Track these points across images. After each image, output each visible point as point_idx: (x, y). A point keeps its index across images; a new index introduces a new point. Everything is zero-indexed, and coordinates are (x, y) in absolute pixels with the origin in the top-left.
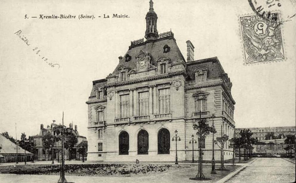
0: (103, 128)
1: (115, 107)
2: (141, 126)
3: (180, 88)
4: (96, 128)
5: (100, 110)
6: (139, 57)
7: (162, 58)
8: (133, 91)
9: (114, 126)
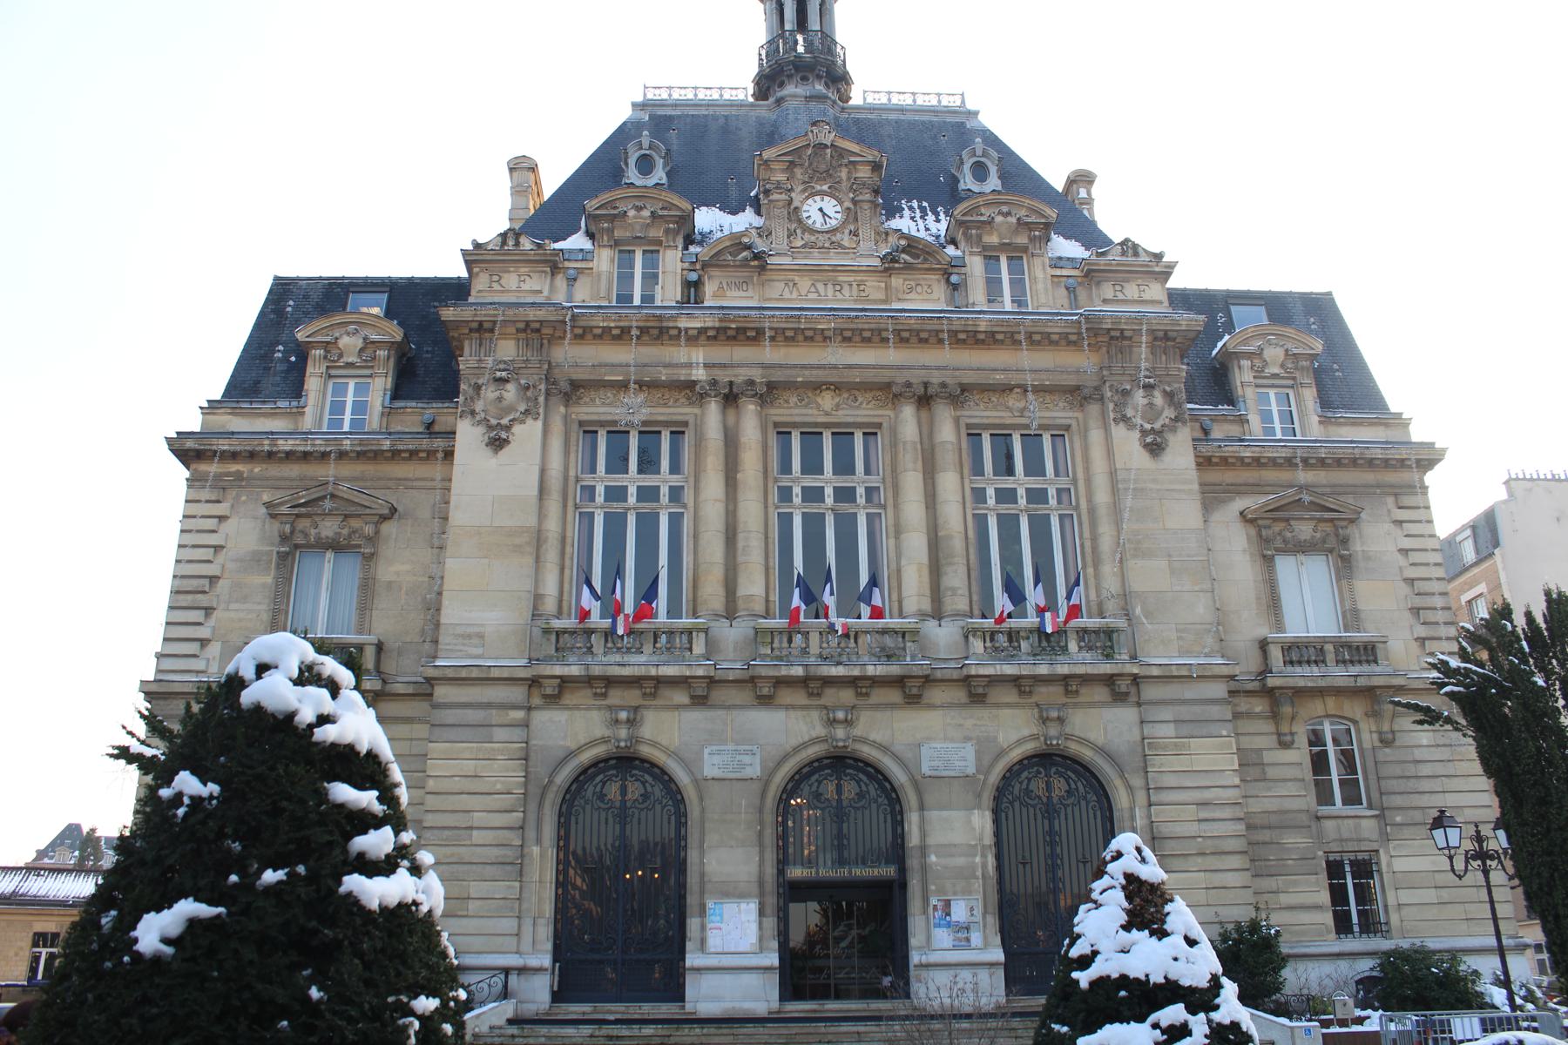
1: (541, 515)
7: (1005, 209)
8: (731, 398)
9: (517, 694)
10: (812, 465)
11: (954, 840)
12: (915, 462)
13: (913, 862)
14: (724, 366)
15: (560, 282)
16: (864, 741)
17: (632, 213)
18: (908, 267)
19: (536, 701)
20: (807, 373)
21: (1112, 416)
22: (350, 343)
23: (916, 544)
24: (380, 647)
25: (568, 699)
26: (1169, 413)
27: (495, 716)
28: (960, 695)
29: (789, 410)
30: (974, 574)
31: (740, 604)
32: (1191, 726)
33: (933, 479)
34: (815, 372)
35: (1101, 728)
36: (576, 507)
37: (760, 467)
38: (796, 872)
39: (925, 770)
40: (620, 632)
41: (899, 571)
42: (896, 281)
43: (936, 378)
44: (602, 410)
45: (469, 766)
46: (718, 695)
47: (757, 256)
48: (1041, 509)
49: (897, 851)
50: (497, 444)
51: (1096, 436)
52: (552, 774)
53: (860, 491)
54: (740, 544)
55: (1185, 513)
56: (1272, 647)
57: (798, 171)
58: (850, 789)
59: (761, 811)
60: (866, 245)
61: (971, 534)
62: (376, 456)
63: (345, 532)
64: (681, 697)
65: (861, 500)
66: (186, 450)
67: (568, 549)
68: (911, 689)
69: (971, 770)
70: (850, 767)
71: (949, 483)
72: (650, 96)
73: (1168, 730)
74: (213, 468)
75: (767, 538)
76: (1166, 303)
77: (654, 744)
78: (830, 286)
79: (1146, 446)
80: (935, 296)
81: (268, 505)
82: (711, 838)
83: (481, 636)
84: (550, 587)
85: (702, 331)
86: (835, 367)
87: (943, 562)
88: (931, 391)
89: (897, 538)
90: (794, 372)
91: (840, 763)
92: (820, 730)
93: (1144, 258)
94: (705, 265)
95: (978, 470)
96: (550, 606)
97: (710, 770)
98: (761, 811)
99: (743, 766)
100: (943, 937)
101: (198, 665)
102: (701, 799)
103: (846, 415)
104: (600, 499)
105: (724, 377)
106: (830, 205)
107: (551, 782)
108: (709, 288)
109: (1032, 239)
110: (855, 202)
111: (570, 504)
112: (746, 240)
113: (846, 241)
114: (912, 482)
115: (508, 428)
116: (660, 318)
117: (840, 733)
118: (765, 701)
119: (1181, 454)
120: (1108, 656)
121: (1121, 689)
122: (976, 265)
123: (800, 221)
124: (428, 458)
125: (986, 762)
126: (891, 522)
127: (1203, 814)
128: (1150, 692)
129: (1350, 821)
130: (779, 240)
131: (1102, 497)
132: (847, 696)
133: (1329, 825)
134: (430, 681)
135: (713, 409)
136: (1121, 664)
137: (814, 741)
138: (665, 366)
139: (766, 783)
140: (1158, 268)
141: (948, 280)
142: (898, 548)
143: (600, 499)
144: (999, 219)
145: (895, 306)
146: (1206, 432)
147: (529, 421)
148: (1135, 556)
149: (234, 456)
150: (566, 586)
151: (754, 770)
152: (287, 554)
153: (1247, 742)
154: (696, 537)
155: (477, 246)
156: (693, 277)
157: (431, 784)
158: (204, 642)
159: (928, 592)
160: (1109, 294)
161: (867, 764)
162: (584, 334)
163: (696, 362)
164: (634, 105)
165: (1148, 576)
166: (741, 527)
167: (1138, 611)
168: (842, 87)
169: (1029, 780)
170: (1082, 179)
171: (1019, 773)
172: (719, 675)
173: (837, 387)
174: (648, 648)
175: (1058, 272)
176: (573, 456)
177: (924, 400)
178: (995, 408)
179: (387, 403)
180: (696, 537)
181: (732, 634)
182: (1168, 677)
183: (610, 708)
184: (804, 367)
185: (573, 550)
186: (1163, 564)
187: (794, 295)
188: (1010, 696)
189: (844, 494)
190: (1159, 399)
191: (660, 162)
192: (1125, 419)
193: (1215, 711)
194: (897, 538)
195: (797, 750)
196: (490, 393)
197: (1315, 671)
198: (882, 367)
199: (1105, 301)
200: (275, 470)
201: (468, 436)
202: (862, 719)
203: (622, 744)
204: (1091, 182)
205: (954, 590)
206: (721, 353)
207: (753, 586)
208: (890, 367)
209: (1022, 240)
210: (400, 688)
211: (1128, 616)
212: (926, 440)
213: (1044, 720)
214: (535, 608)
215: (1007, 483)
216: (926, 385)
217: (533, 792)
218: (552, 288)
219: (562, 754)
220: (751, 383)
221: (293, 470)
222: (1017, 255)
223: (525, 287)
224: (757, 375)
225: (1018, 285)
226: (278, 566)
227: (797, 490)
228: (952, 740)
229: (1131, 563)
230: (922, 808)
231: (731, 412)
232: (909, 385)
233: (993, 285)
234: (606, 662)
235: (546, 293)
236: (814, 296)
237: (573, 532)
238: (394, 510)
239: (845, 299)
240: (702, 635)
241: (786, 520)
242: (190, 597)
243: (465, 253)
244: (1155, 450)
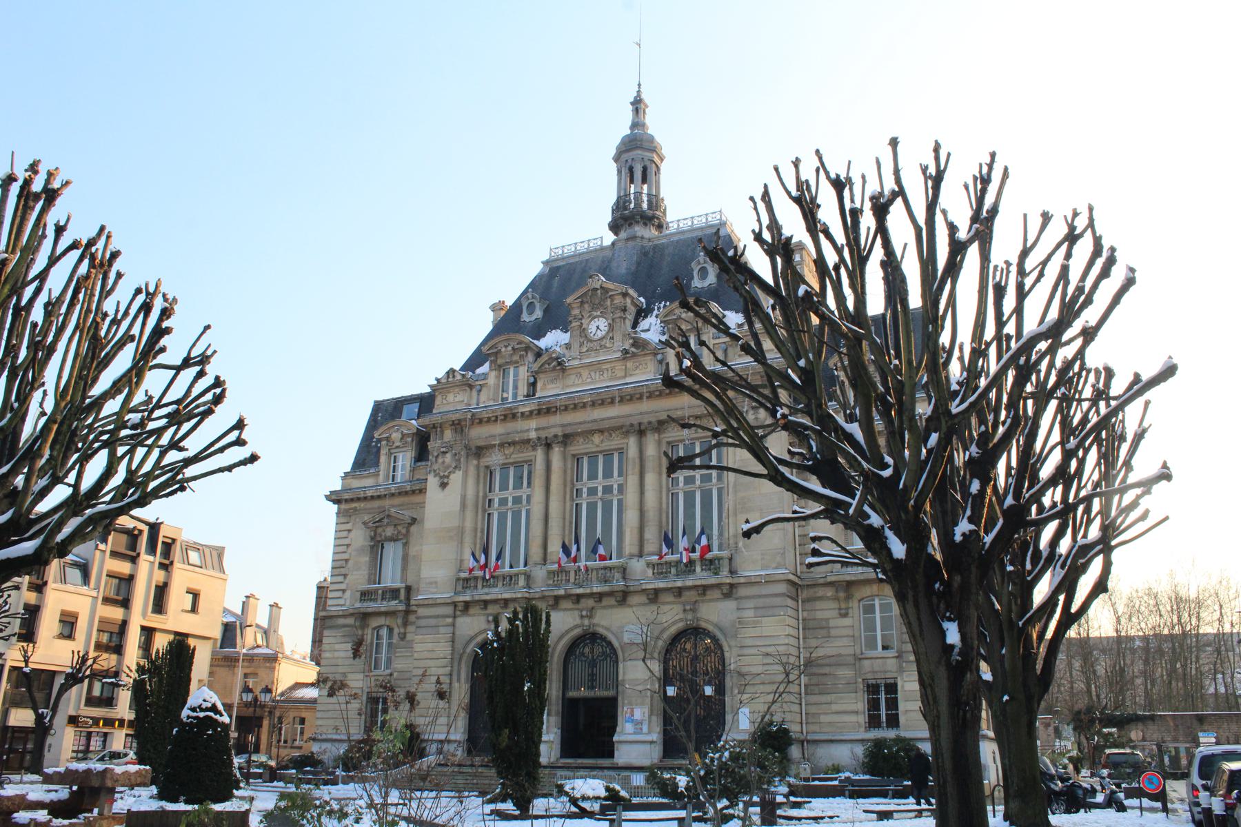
1: (464, 520)
2: (582, 617)
5: (389, 531)
6: (582, 303)
10: (593, 476)
11: (638, 677)
13: (620, 688)
14: (544, 428)
15: (474, 393)
16: (598, 625)
18: (634, 355)
19: (458, 613)
22: (396, 436)
23: (631, 517)
25: (472, 611)
27: (441, 621)
28: (643, 599)
29: (578, 447)
32: (764, 611)
35: (715, 613)
38: (572, 694)
39: (626, 640)
42: (630, 364)
43: (645, 420)
48: (707, 486)
49: (616, 684)
50: (443, 485)
53: (615, 486)
57: (586, 306)
62: (406, 493)
65: (615, 492)
68: (623, 597)
71: (650, 478)
74: (344, 506)
86: (595, 421)
92: (578, 621)
94: (537, 372)
100: (629, 727)
103: (607, 445)
105: (543, 434)
106: (603, 323)
108: (539, 385)
114: (632, 481)
120: (716, 574)
121: (730, 591)
127: (766, 661)
128: (742, 592)
130: (575, 352)
132: (590, 603)
136: (725, 578)
137: (576, 627)
145: (628, 380)
155: (438, 380)
163: (531, 428)
172: (532, 596)
173: (601, 431)
174: (500, 584)
181: (539, 573)
182: (750, 583)
184: (581, 423)
188: (670, 598)
189: (608, 489)
191: (538, 305)
193: (778, 601)
195: (567, 632)
201: (433, 482)
206: (544, 421)
216: (640, 424)
217: (455, 658)
218: (471, 397)
220: (556, 436)
227: (585, 490)
232: (632, 425)
234: (483, 593)
238: (414, 520)
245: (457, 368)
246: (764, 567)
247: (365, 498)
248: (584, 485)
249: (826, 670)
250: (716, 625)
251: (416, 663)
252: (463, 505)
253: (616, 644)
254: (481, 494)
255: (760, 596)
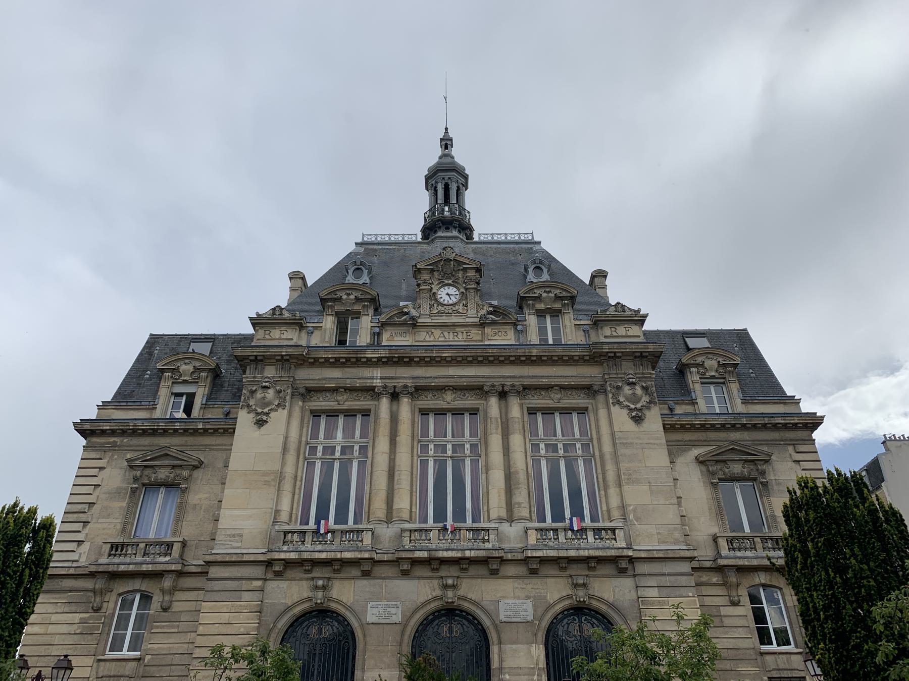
0: (167, 583)
1: (283, 464)
3: (648, 413)
4: (114, 576)
6: (432, 271)
7: (548, 290)
8: (395, 396)
9: (259, 571)
12: (497, 429)
14: (392, 378)
16: (464, 599)
17: (344, 297)
18: (493, 323)
19: (270, 575)
20: (436, 380)
21: (611, 401)
23: (498, 476)
24: (184, 544)
25: (290, 573)
26: (646, 399)
27: (245, 585)
30: (533, 494)
31: (394, 513)
33: (508, 438)
34: (441, 380)
35: (611, 590)
36: (305, 459)
37: (409, 433)
39: (502, 618)
40: (322, 532)
41: (488, 492)
42: (487, 330)
43: (509, 382)
44: (323, 403)
45: (225, 617)
46: (378, 570)
47: (413, 318)
50: (260, 423)
51: (602, 413)
52: (275, 623)
54: (396, 478)
55: (659, 457)
56: (720, 540)
58: (457, 629)
59: (400, 644)
60: (472, 312)
61: (530, 470)
63: (172, 475)
64: (355, 572)
66: (85, 429)
67: (298, 483)
69: (530, 618)
70: (457, 615)
71: (517, 441)
72: (365, 239)
73: (654, 592)
75: (412, 474)
76: (642, 337)
77: (338, 602)
78: (451, 334)
79: (633, 418)
80: (508, 337)
81: (128, 461)
82: (370, 663)
83: (241, 535)
84: (285, 506)
85: (379, 359)
86: (453, 377)
87: (513, 487)
88: (506, 389)
89: (487, 473)
90: (430, 380)
91: (450, 612)
92: (438, 592)
93: (628, 312)
95: (534, 433)
96: (284, 517)
97: (371, 618)
98: (400, 644)
99: (390, 615)
101: (74, 557)
102: (365, 636)
104: (319, 454)
105: (390, 383)
106: (452, 290)
107: (274, 626)
109: (564, 305)
110: (466, 289)
111: (301, 456)
112: (405, 310)
113: (460, 308)
114: (496, 441)
115: (267, 414)
116: (357, 352)
117: (450, 594)
118: (405, 574)
119: (654, 421)
121: (622, 565)
122: (532, 320)
123: (436, 300)
124: (224, 433)
125: (539, 614)
126: (484, 464)
129: (784, 656)
130: (425, 309)
131: (607, 448)
133: (768, 658)
134: (208, 563)
135: (385, 402)
138: (359, 379)
139: (404, 625)
140: (639, 319)
141: (516, 329)
142: (487, 478)
143: (319, 454)
144: (544, 295)
146: (671, 410)
147: (280, 410)
148: (627, 483)
149: (113, 433)
150: (295, 506)
151: (398, 618)
152: (137, 488)
153: (708, 601)
154: (371, 475)
156: (377, 330)
157: (201, 630)
158: (80, 542)
159: (504, 506)
160: (608, 333)
161: (468, 614)
162: (316, 363)
163: (376, 376)
164: (356, 244)
165: (636, 495)
166: (397, 468)
167: (631, 517)
168: (468, 232)
169: (569, 624)
170: (600, 275)
171: (562, 620)
175: (578, 322)
176: (305, 429)
177: (503, 395)
178: (543, 399)
179: (204, 402)
180: (371, 475)
181: (387, 533)
183: (313, 579)
185: (301, 485)
186: (646, 487)
187: (432, 339)
188: (553, 571)
190: (639, 391)
192: (619, 403)
193: (684, 580)
194: (487, 473)
195: (424, 605)
196: (259, 395)
197: (749, 554)
198: (479, 377)
199: (605, 337)
200: (135, 441)
201: (244, 419)
202: (464, 585)
203: (319, 601)
204: (605, 277)
205: (519, 504)
206: (390, 371)
207: (402, 503)
208: (484, 377)
209: (557, 306)
210: (193, 569)
211: (625, 519)
212: (503, 415)
213: (576, 586)
214: (275, 518)
215: (552, 440)
216: (503, 386)
219: (282, 608)
220: (406, 387)
221: (146, 441)
222: (556, 314)
223: (283, 337)
224: (409, 382)
225: (556, 331)
226: (130, 497)
228: (519, 598)
229: (626, 488)
230: (500, 643)
231: (395, 403)
232: (493, 386)
233: (542, 331)
235: (295, 340)
236: (443, 339)
237: (302, 473)
238: (201, 463)
239: (459, 338)
240: (370, 533)
241: (424, 464)
242: (75, 515)
243: (251, 319)
244: (638, 419)
245: (284, 305)
246: (661, 542)
247: (134, 433)
248: (431, 441)
249: (727, 665)
250: (611, 605)
251: (200, 641)
252: (285, 449)
253: (486, 622)
254: (304, 439)
255: (663, 575)
